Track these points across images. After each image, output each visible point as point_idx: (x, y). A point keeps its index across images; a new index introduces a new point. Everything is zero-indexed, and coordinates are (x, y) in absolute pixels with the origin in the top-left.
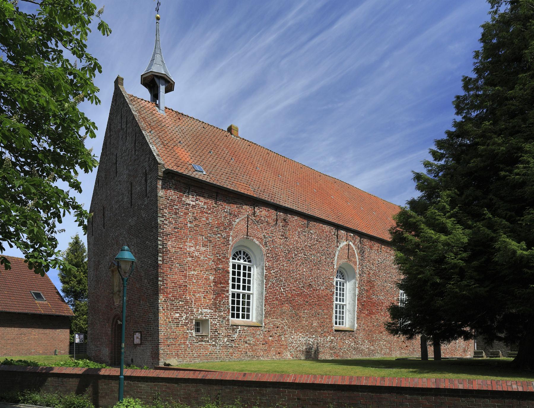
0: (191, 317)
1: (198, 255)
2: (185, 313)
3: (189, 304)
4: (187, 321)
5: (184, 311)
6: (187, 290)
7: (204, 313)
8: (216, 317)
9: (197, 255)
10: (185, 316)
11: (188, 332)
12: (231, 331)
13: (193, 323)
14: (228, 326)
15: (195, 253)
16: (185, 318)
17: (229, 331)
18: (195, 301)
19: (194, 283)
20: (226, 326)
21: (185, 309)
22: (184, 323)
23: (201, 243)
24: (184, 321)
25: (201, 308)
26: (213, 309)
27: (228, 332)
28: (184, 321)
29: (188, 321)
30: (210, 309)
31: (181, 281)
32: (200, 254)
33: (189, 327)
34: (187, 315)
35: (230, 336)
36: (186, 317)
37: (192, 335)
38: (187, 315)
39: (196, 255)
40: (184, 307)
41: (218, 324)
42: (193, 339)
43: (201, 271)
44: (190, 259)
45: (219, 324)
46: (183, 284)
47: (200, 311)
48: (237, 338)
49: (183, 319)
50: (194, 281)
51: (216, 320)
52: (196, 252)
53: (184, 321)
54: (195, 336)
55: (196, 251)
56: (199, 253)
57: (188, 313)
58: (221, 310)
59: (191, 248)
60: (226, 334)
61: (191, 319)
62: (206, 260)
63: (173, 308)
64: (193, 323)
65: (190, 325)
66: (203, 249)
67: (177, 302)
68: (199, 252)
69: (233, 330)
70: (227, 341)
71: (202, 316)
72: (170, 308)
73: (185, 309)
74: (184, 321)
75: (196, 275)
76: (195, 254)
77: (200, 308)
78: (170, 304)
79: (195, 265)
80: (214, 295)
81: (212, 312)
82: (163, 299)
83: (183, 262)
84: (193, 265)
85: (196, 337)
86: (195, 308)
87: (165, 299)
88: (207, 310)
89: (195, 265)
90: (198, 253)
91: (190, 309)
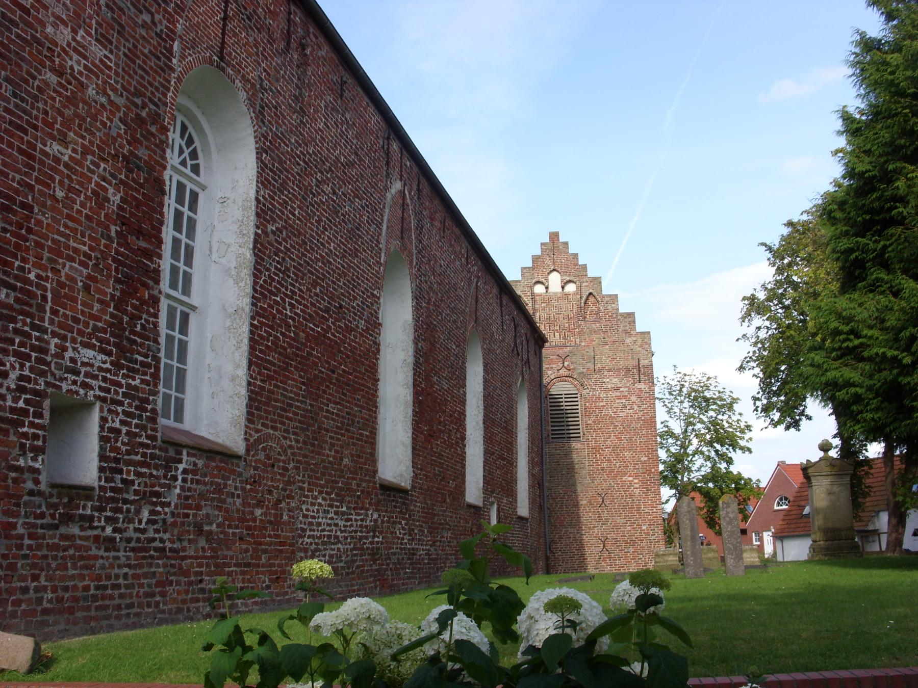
0: (36, 383)
1: (80, 73)
2: (17, 354)
4: (21, 404)
5: (12, 342)
6: (30, 231)
7: (83, 370)
8: (120, 398)
9: (76, 68)
10: (17, 372)
11: (22, 462)
12: (161, 473)
13: (41, 416)
14: (154, 447)
15: (71, 59)
16: (13, 386)
17: (155, 473)
19: (57, 201)
20: (147, 446)
21: (17, 331)
22: (13, 410)
23: (94, 22)
24: (9, 403)
25: (74, 341)
26: (109, 354)
27: (151, 475)
28: (9, 403)
29: (27, 401)
30: (102, 351)
31: (13, 180)
32: (86, 67)
33: (25, 435)
34: (22, 366)
35: (158, 495)
36: (21, 378)
37: (37, 482)
38: (22, 366)
39: (72, 68)
40: (14, 321)
41: (124, 429)
42: (40, 506)
43: (86, 151)
44: (52, 78)
45: (128, 433)
46: (17, 191)
47: (69, 354)
48: (176, 506)
49: (8, 389)
50: (60, 194)
51: (120, 409)
52: (75, 57)
53: (9, 397)
54: (48, 490)
55: (75, 50)
56: (83, 61)
57: (28, 357)
58: (136, 361)
59: (62, 27)
60: (146, 485)
61: (36, 393)
62: (102, 105)
64: (41, 416)
65: (32, 425)
66: (97, 51)
68: (85, 58)
69: (168, 468)
70: (149, 522)
71: (75, 382)
73: (17, 331)
74: (9, 397)
75: (66, 165)
76: (70, 63)
77: (69, 335)
79: (67, 112)
80: (117, 281)
81: (108, 366)
83: (26, 82)
84: (61, 114)
85: (51, 496)
86: (54, 334)
88: (91, 353)
89: (67, 112)
90: (79, 63)
91: (37, 339)
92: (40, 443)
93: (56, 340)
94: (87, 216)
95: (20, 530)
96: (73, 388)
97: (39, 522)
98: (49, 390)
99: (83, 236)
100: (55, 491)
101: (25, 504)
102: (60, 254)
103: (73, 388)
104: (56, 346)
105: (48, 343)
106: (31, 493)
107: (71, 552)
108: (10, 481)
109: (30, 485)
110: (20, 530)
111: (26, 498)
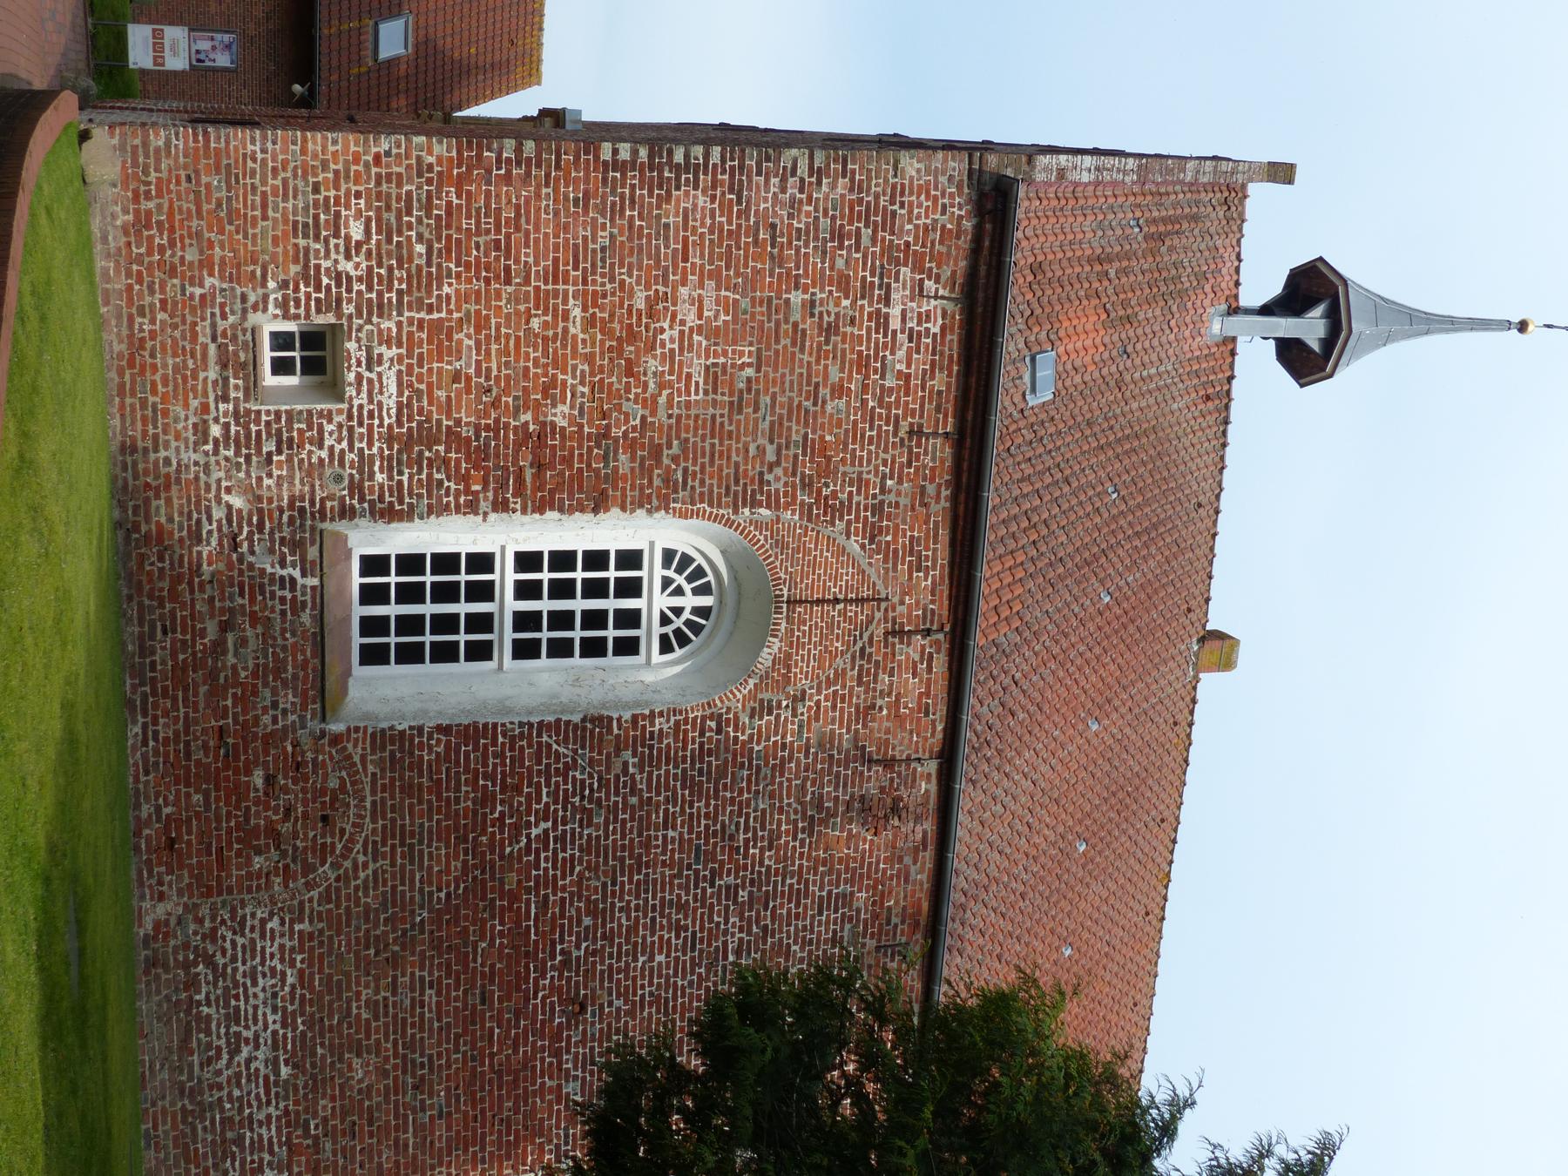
0: (349, 301)
3: (416, 294)
4: (325, 281)
11: (271, 284)
18: (436, 327)
24: (325, 264)
25: (400, 359)
28: (325, 264)
33: (296, 290)
37: (255, 308)
40: (400, 267)
42: (233, 313)
57: (370, 289)
61: (339, 301)
63: (388, 208)
64: (319, 311)
67: (422, 229)
72: (389, 195)
77: (403, 351)
78: (409, 193)
82: (431, 159)
85: (244, 331)
86: (399, 324)
87: (430, 167)
92: (292, 311)
93: (395, 330)
94: (527, 369)
95: (208, 281)
96: (353, 361)
97: (217, 311)
98: (344, 322)
99: (507, 364)
100: (249, 336)
101: (233, 289)
102: (478, 330)
103: (353, 361)
104: (389, 329)
105: (390, 317)
106: (244, 298)
107: (190, 363)
108: (252, 268)
109: (252, 298)
110: (208, 281)
111: (239, 291)
